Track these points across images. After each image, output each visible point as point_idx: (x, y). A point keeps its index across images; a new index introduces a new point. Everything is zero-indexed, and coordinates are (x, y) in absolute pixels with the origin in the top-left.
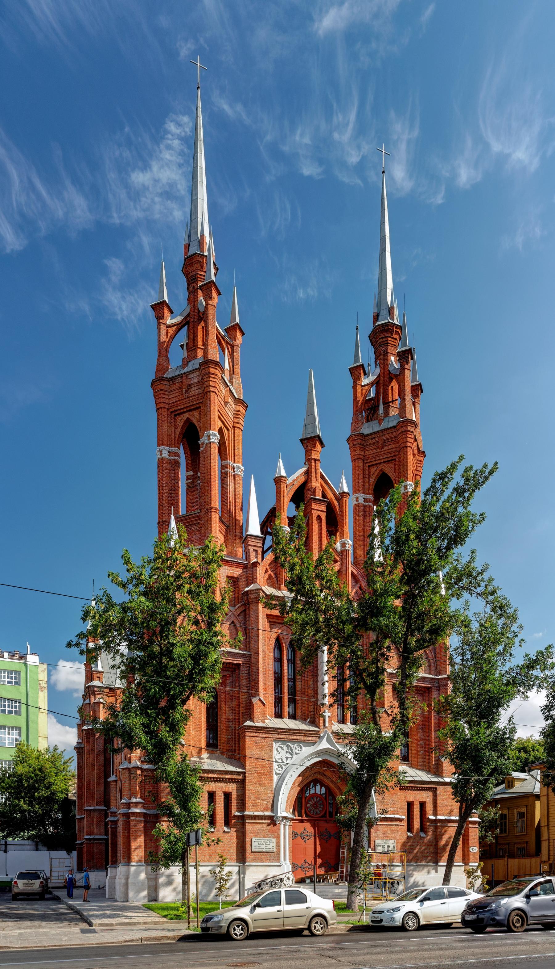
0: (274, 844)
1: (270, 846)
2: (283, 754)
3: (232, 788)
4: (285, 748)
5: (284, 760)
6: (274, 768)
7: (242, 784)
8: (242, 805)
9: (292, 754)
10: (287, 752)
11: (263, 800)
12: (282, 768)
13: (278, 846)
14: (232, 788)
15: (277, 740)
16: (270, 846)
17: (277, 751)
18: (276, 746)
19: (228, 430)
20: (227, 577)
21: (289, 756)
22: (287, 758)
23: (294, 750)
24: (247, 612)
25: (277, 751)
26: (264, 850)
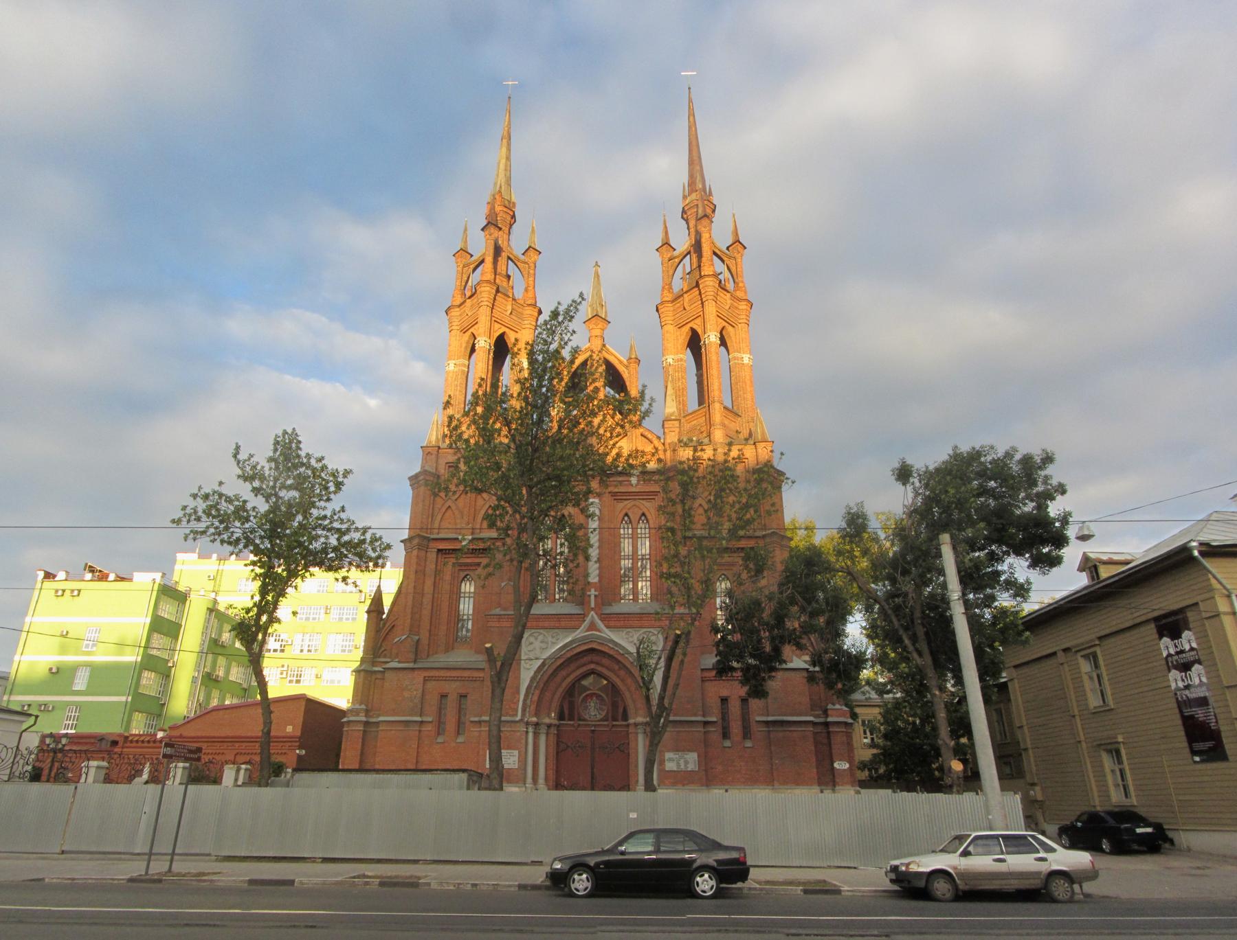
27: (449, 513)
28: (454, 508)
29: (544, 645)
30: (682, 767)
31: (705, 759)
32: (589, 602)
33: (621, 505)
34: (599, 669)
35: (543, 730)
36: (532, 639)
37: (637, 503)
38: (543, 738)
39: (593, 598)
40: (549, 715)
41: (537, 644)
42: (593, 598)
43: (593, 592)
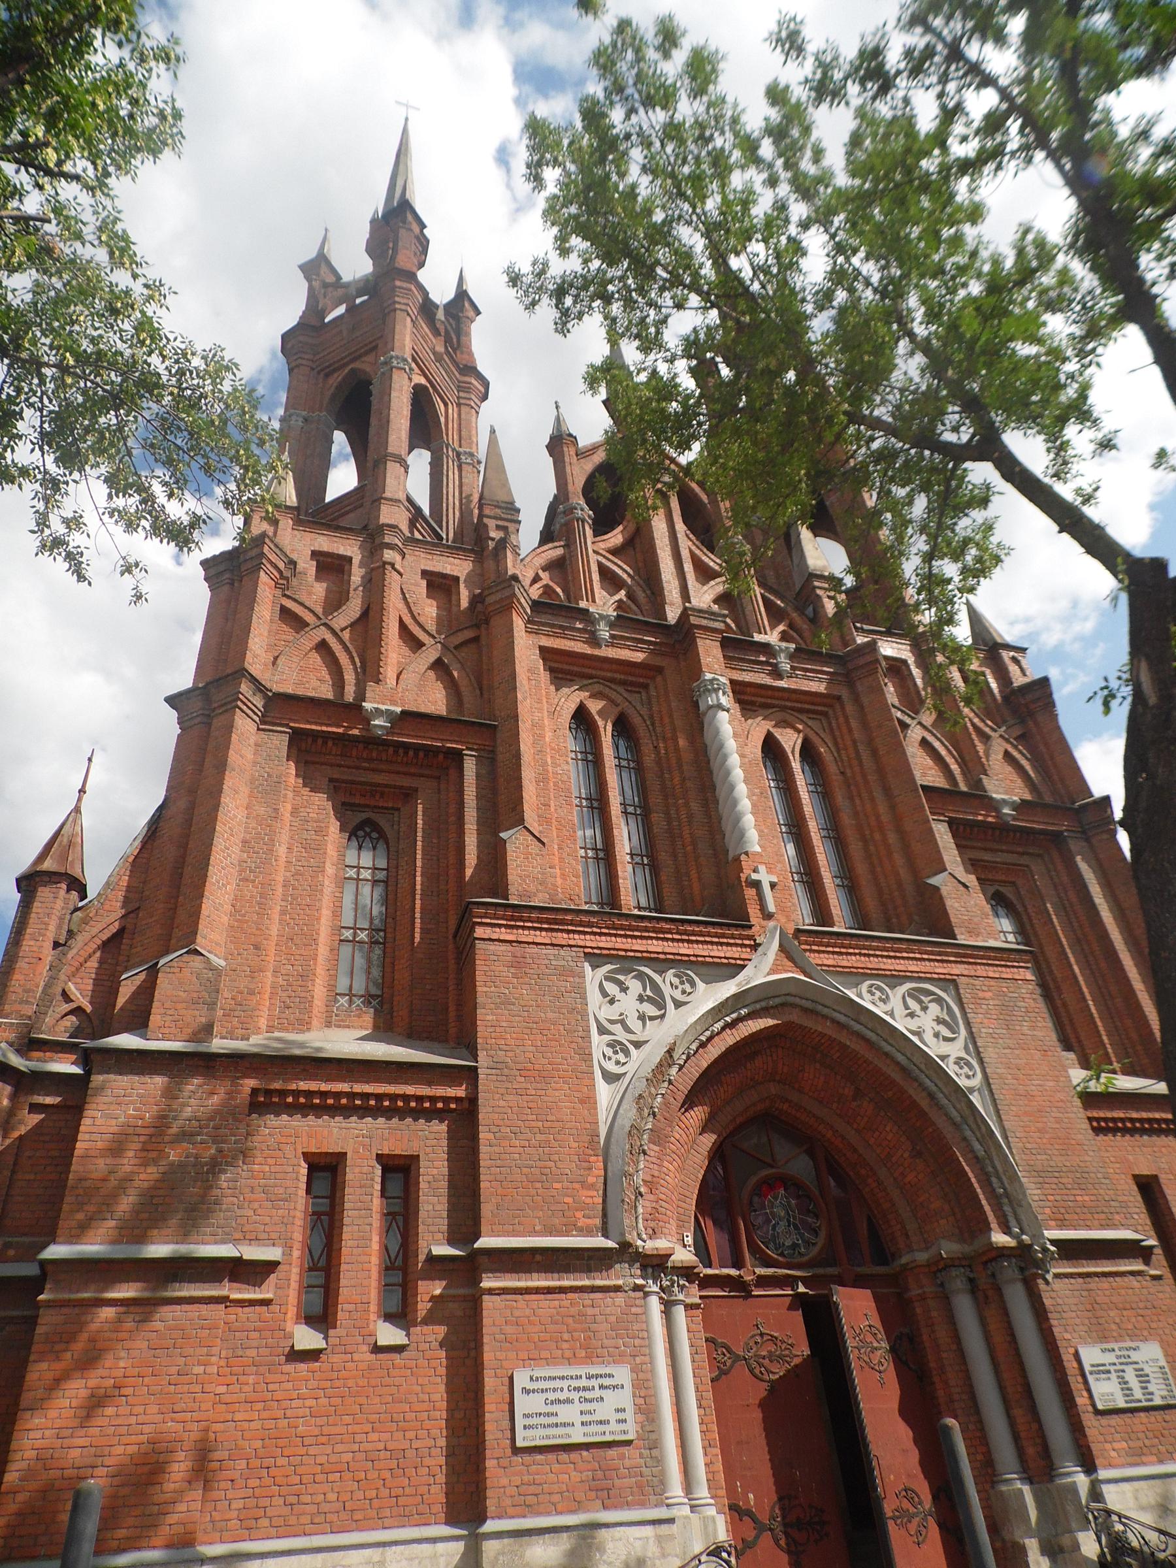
0: (625, 1398)
1: (604, 1411)
2: (629, 1004)
3: (428, 1142)
4: (635, 987)
5: (634, 1023)
6: (597, 1055)
7: (464, 1120)
8: (465, 1218)
9: (661, 1006)
10: (641, 999)
12: (627, 1053)
13: (647, 1410)
14: (428, 1142)
15: (596, 958)
16: (604, 1411)
17: (604, 994)
19: (446, 405)
21: (651, 1010)
22: (642, 1017)
23: (667, 990)
24: (483, 641)
25: (604, 994)
26: (577, 1437)
30: (1138, 1394)
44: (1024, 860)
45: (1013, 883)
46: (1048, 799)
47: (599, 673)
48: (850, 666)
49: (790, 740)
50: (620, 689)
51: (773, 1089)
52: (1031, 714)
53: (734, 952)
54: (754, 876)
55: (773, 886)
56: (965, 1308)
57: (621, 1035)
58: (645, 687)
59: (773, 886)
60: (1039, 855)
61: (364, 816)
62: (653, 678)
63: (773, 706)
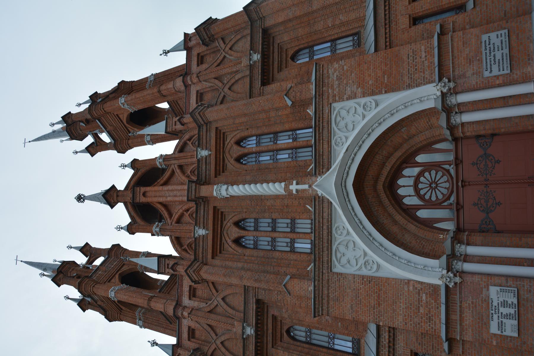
11: (420, 301)
18: (338, 268)
20: (190, 299)
27: (227, 344)
28: (223, 338)
29: (351, 245)
31: (488, 24)
32: (304, 191)
33: (229, 166)
34: (383, 178)
35: (462, 249)
36: (344, 260)
37: (227, 151)
38: (472, 250)
39: (300, 187)
40: (444, 240)
41: (350, 254)
42: (300, 187)
43: (294, 187)
44: (276, 46)
45: (286, 50)
46: (248, 31)
47: (219, 231)
48: (202, 123)
49: (237, 151)
50: (225, 223)
51: (380, 186)
52: (213, 35)
53: (326, 205)
54: (294, 192)
55: (297, 184)
56: (467, 118)
57: (361, 261)
58: (222, 212)
59: (297, 184)
60: (273, 37)
61: (285, 334)
62: (218, 210)
63: (223, 157)
